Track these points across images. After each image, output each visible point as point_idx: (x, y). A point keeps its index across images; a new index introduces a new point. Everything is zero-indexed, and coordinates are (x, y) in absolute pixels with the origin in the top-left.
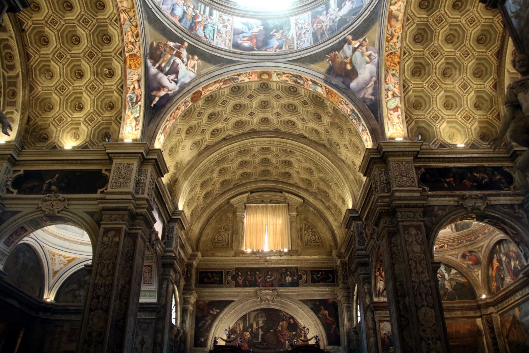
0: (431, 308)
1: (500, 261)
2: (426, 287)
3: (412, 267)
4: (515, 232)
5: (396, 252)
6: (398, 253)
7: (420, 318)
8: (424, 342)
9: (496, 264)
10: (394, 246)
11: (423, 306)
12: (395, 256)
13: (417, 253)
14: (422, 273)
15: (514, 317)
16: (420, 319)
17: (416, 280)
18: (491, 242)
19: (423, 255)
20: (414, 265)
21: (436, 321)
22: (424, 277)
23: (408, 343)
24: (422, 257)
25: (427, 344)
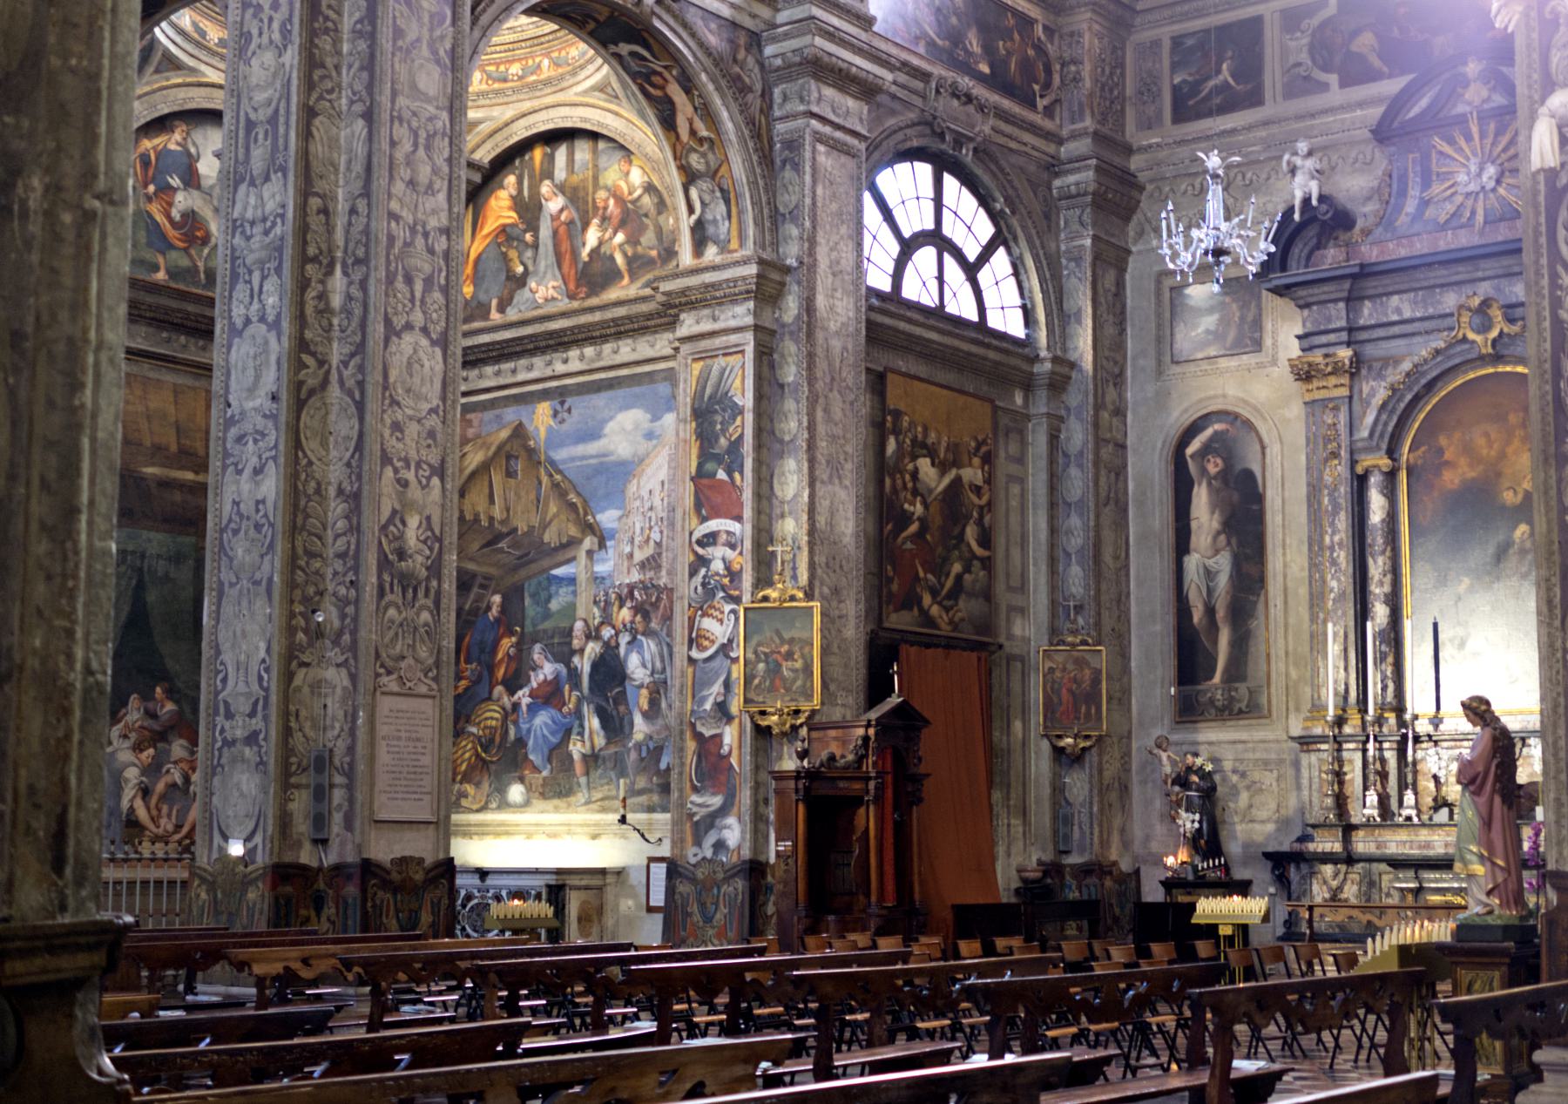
0: (434, 343)
1: (529, 209)
2: (431, 251)
3: (399, 155)
4: (704, 133)
5: (329, 62)
6: (337, 67)
7: (393, 374)
8: (389, 472)
9: (500, 207)
10: (327, 31)
11: (409, 327)
12: (322, 78)
13: (428, 100)
14: (430, 190)
15: (519, 432)
16: (391, 380)
17: (404, 214)
18: (523, 122)
19: (445, 115)
20: (407, 146)
21: (444, 399)
22: (434, 212)
23: (310, 463)
24: (439, 124)
25: (398, 481)
